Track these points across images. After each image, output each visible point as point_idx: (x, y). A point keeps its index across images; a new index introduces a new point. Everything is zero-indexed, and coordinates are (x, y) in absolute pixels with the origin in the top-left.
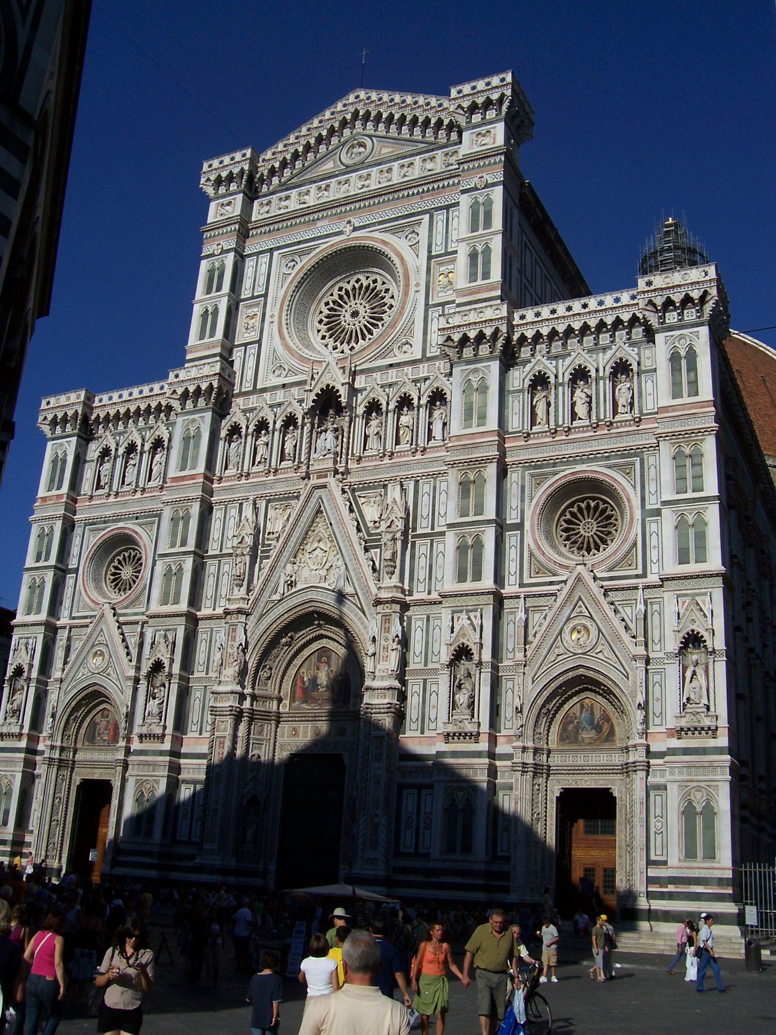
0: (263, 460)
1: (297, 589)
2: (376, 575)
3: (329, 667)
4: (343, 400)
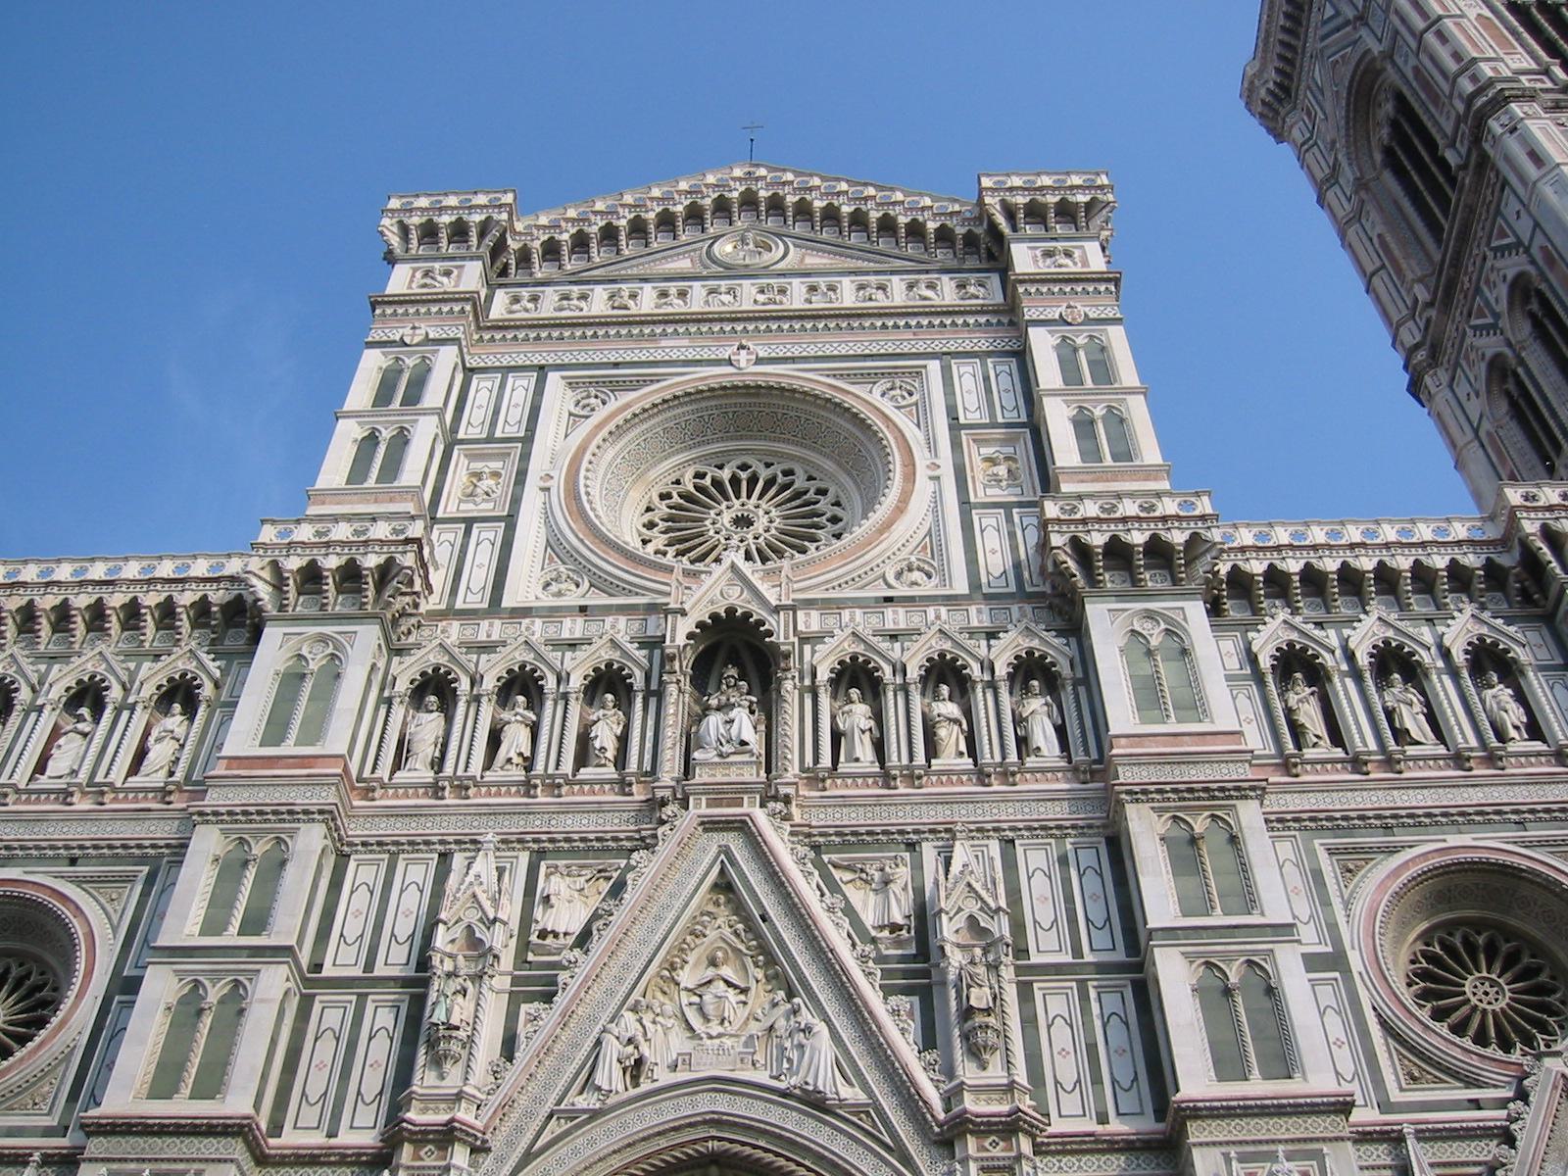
0: (516, 760)
1: (656, 1085)
2: (929, 1057)
4: (779, 638)
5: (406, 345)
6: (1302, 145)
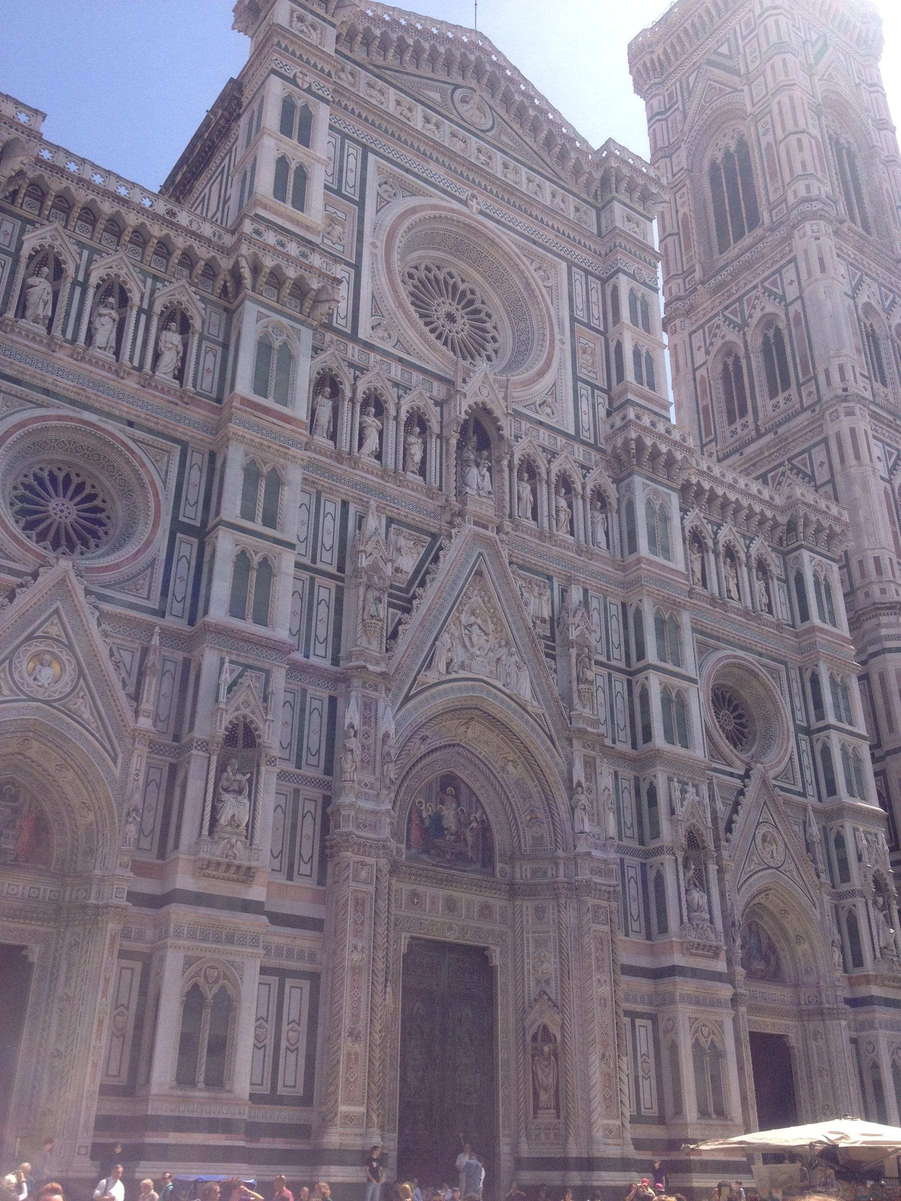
3: (459, 805)
4: (506, 433)
5: (297, 86)
6: (658, 114)
